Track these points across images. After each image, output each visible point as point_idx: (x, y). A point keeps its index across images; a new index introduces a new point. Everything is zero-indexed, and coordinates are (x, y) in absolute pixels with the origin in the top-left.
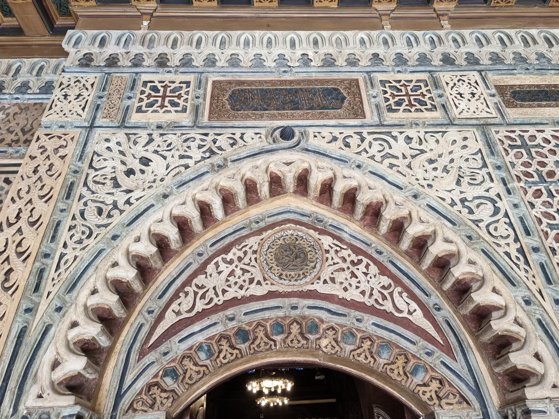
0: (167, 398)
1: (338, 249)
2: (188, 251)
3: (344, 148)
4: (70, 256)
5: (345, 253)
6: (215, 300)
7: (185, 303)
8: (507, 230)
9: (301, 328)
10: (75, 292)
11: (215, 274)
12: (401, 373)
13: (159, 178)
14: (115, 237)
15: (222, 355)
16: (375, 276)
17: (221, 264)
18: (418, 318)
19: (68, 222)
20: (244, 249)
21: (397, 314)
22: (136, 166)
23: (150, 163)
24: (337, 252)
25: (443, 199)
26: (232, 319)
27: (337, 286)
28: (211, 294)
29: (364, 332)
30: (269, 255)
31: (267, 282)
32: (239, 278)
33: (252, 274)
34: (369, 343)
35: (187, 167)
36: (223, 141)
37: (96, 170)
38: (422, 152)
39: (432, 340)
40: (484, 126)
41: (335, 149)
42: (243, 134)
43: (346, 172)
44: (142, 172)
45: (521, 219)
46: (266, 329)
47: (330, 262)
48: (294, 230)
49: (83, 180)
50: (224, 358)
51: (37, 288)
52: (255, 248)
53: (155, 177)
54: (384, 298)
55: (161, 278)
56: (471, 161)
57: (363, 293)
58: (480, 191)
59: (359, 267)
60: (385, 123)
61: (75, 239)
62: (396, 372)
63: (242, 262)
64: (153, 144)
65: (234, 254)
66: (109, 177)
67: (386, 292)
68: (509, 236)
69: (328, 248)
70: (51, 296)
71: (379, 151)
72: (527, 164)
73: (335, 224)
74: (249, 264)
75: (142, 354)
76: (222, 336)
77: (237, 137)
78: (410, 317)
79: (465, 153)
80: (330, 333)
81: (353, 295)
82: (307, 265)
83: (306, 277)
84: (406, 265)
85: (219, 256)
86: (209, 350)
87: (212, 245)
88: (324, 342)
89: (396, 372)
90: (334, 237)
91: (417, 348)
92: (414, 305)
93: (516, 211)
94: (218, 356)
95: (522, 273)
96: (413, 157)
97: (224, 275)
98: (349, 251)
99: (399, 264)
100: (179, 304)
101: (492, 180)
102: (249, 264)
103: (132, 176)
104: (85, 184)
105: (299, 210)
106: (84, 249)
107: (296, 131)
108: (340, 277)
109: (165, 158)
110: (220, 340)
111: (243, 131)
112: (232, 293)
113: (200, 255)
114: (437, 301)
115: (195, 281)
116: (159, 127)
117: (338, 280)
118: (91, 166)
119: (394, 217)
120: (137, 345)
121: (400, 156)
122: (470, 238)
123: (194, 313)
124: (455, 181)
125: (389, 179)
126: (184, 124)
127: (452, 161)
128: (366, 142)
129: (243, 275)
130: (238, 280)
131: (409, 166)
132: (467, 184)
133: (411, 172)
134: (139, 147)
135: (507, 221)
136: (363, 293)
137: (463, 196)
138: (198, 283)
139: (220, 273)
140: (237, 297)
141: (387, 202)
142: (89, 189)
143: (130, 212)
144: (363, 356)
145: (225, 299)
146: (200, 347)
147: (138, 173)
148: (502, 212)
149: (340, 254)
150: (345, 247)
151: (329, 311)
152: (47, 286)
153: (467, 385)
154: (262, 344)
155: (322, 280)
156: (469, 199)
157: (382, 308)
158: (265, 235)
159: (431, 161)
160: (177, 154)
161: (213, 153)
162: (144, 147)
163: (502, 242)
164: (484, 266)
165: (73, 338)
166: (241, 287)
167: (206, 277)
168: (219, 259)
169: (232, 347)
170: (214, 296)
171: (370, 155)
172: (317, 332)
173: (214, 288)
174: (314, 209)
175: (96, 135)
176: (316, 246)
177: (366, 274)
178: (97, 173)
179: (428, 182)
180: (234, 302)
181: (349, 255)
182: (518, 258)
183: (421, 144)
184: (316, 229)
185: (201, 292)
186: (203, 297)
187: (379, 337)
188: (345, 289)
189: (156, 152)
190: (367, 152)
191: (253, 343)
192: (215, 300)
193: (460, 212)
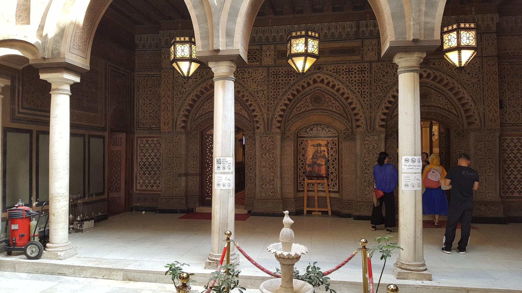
7: (200, 112)
18: (246, 115)
19: (175, 96)
35: (197, 81)
40: (268, 67)
58: (261, 88)
72: (275, 80)
76: (208, 119)
159: (252, 80)
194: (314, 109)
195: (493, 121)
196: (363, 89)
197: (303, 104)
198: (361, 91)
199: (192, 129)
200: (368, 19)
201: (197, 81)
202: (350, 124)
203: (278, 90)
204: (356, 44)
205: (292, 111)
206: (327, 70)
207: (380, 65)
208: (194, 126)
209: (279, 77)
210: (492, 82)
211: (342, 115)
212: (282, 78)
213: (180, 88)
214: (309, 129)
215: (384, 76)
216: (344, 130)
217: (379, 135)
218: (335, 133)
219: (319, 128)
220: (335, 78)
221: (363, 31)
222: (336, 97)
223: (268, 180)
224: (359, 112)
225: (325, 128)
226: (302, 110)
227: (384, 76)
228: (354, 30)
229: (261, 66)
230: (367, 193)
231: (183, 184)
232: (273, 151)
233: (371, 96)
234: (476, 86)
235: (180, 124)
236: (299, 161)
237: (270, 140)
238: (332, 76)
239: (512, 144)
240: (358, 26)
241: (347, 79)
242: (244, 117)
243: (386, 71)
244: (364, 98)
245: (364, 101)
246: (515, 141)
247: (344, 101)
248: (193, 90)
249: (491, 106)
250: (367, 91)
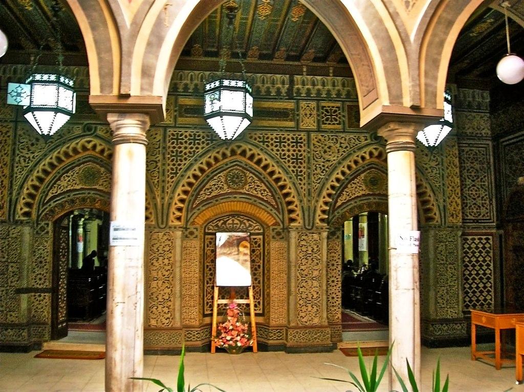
19: (16, 165)
28: (62, 188)
45: (164, 170)
61: (19, 170)
76: (66, 201)
88: (97, 205)
90: (105, 167)
113: (59, 173)
152: (14, 187)
176: (99, 172)
180: (70, 191)
194: (231, 193)
195: (455, 216)
196: (300, 167)
197: (215, 185)
198: (297, 170)
200: (304, 73)
202: (281, 217)
203: (179, 162)
204: (290, 105)
205: (198, 194)
206: (251, 137)
207: (320, 137)
209: (181, 143)
210: (452, 167)
211: (269, 203)
212: (185, 145)
213: (25, 151)
214: (222, 221)
215: (325, 152)
216: (272, 225)
217: (320, 233)
218: (258, 229)
219: (236, 221)
220: (262, 150)
221: (298, 89)
222: (262, 177)
223: (160, 299)
224: (294, 200)
225: (245, 221)
226: (213, 194)
227: (325, 152)
228: (287, 86)
230: (303, 314)
231: (24, 305)
232: (170, 255)
233: (309, 178)
234: (435, 171)
235: (21, 209)
236: (207, 270)
237: (165, 238)
238: (258, 147)
239: (473, 246)
240: (292, 82)
241: (278, 153)
243: (329, 145)
244: (301, 180)
245: (300, 184)
246: (477, 241)
247: (273, 183)
248: (45, 155)
249: (451, 198)
250: (304, 170)
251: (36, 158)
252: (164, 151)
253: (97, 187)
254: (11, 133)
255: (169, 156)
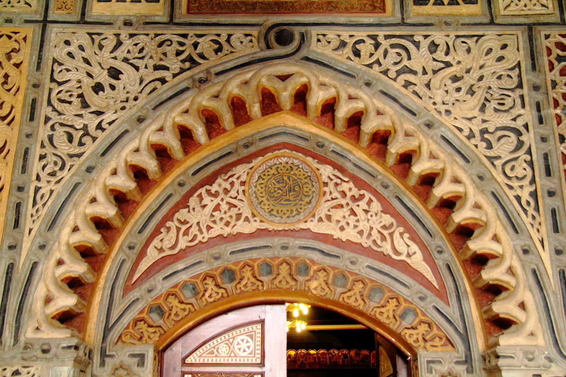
0: (155, 332)
1: (339, 181)
2: (168, 181)
3: (353, 57)
4: (45, 190)
5: (345, 187)
6: (200, 238)
7: (167, 239)
8: (525, 169)
9: (290, 269)
10: (56, 230)
11: (198, 208)
12: (391, 316)
13: (132, 97)
14: (89, 170)
15: (207, 294)
16: (376, 214)
17: (204, 195)
18: (418, 261)
19: (37, 151)
20: (231, 180)
21: (394, 257)
22: (104, 78)
23: (120, 76)
24: (336, 184)
25: (460, 130)
26: (217, 258)
27: (333, 225)
28: (194, 230)
29: (357, 274)
30: (259, 187)
31: (256, 218)
32: (225, 213)
33: (239, 209)
34: (361, 285)
35: (163, 81)
36: (205, 45)
37: (60, 84)
38: (448, 65)
39: (428, 284)
41: (342, 58)
42: (230, 36)
43: (352, 91)
44: (113, 87)
46: (253, 269)
47: (328, 197)
48: (289, 157)
49: (46, 97)
50: (210, 296)
51: (17, 224)
52: (243, 178)
53: (128, 95)
54: (384, 238)
55: (140, 211)
56: (505, 78)
57: (361, 233)
58: (505, 120)
59: (360, 203)
60: (408, 21)
61: (48, 170)
62: (385, 315)
63: (229, 195)
64: (122, 48)
65: (220, 185)
66: (75, 94)
67: (385, 233)
68: (525, 177)
69: (327, 180)
70: (33, 233)
71: (396, 64)
73: (338, 150)
74: (236, 198)
75: (127, 289)
77: (223, 40)
78: (408, 261)
79: (501, 68)
80: (322, 274)
81: (350, 235)
82: (301, 200)
83: (299, 213)
84: (413, 202)
85: (203, 187)
86: (194, 289)
87: (194, 174)
88: (314, 284)
89: (385, 315)
90: (335, 166)
91: (410, 291)
92: (414, 247)
93: (543, 145)
94: (204, 295)
95: (527, 220)
96: (435, 72)
97: (209, 209)
98: (351, 185)
99: (405, 200)
100: (161, 240)
101: (523, 106)
102: (236, 198)
103: (101, 93)
104: (49, 103)
105: (296, 132)
106: (58, 182)
107: (297, 31)
108: (338, 214)
109: (137, 69)
110: (205, 279)
111: (229, 30)
112: (217, 230)
113: (181, 185)
114: (440, 243)
115: (177, 215)
116: (128, 24)
117: (335, 218)
118: (53, 80)
119: (401, 151)
120: (121, 282)
121: (420, 71)
122: (481, 178)
123: (176, 251)
124: (480, 105)
125: (402, 101)
126: (157, 19)
127: (481, 78)
128: (381, 50)
129: (229, 209)
130: (223, 216)
131: (428, 86)
132: (492, 111)
133: (429, 93)
134: (106, 53)
135: (528, 158)
136: (361, 233)
137: (484, 126)
138: (180, 218)
139: (204, 206)
140: (222, 235)
141: (395, 131)
142: (54, 110)
143: (103, 138)
144: (353, 299)
145: (211, 236)
146: (185, 285)
147: (107, 88)
148: (525, 148)
149: (340, 188)
150: (346, 179)
151: (322, 252)
152: (27, 223)
153: (456, 329)
154: (249, 285)
155: (317, 217)
156: (490, 130)
157: (379, 250)
158: (256, 162)
159: (455, 79)
160: (151, 63)
161: (194, 63)
162: (112, 52)
163: (515, 184)
164: (490, 211)
165: (60, 276)
166: (227, 224)
167: (189, 212)
168: (203, 191)
169: (217, 285)
170: (198, 233)
171: (383, 68)
172: (307, 274)
173: (198, 223)
174: (315, 130)
175: (53, 35)
177: (366, 211)
178: (61, 88)
179: (447, 107)
181: (350, 189)
182: (528, 203)
183: (447, 54)
184: (314, 156)
185: (184, 228)
186: (186, 233)
187: (372, 281)
188: (342, 229)
189: (126, 60)
190: (380, 65)
191: (239, 283)
192: (200, 238)
193: (476, 146)
199: (114, 335)
201: (163, 81)
208: (127, 319)
213: (70, 112)
229: (492, 23)
235: (48, 300)
242: (404, 267)
251: (109, 129)
252: (539, 97)
253: (314, 226)
254: (26, 55)
255: (558, 111)
